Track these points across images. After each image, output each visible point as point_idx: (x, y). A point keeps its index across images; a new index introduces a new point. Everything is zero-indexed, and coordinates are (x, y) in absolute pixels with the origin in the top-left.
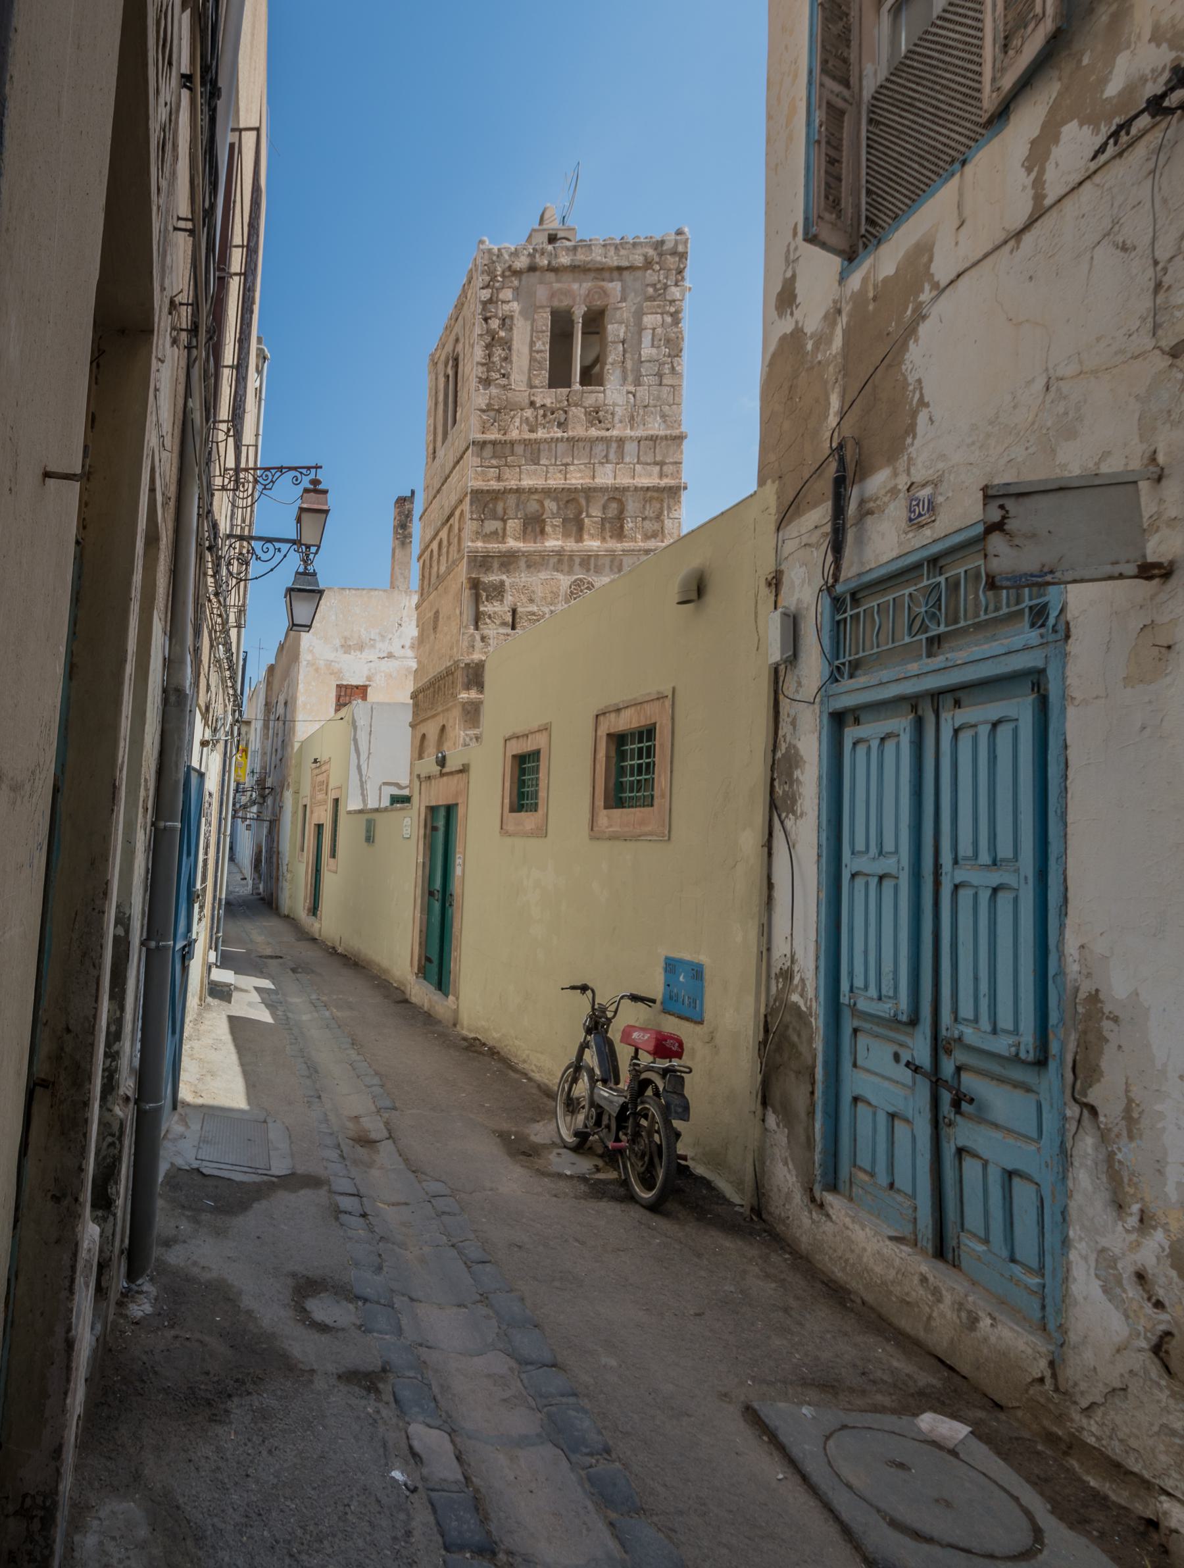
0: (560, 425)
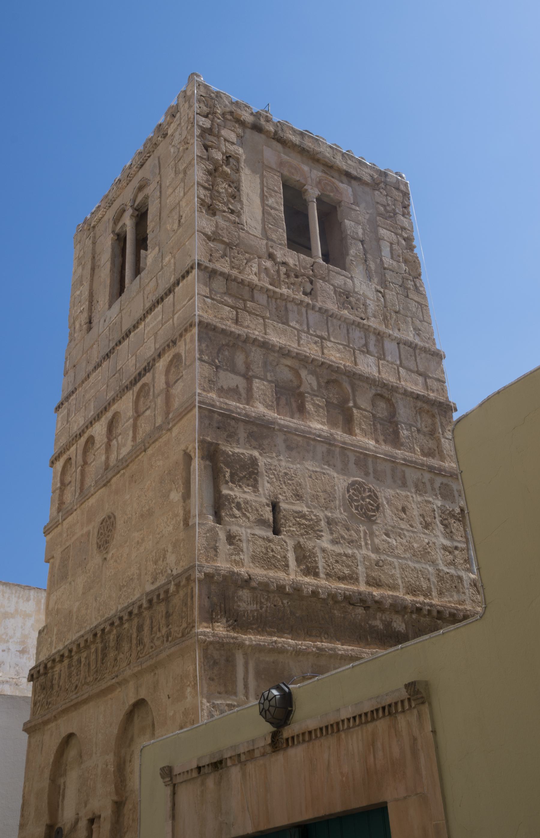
0: (305, 293)
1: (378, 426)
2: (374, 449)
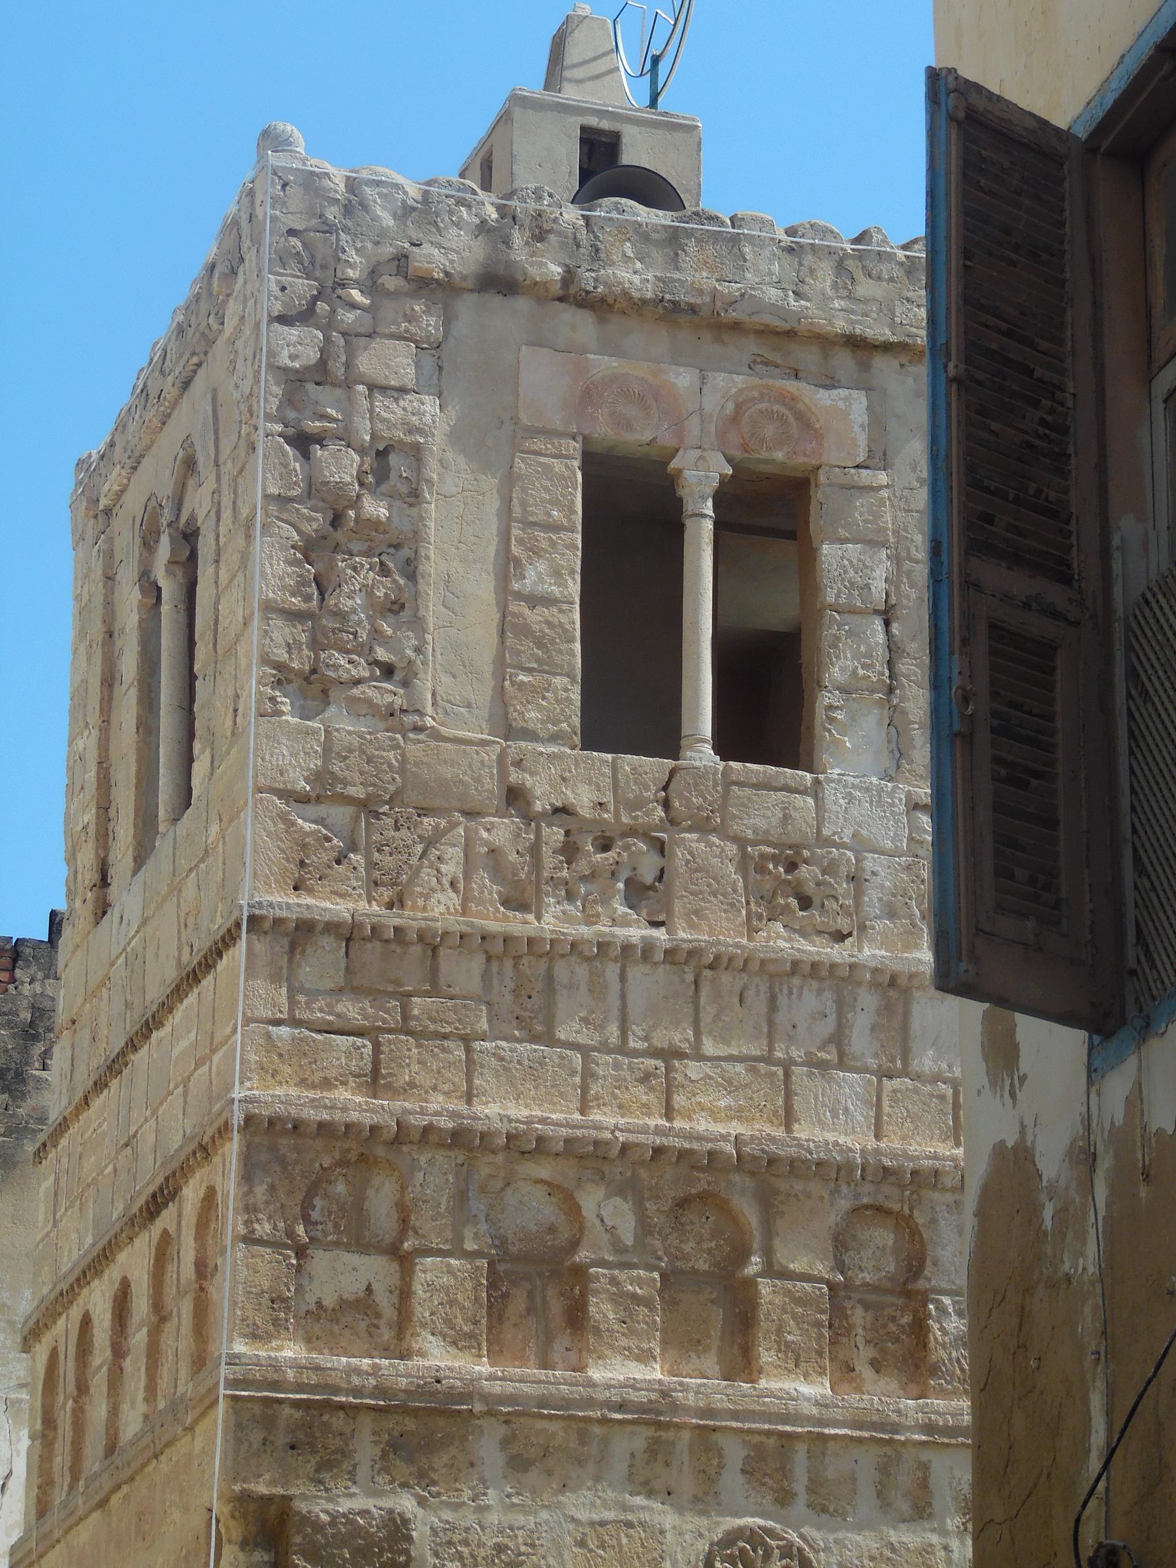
0: (636, 893)
1: (858, 1316)
2: (815, 1411)
